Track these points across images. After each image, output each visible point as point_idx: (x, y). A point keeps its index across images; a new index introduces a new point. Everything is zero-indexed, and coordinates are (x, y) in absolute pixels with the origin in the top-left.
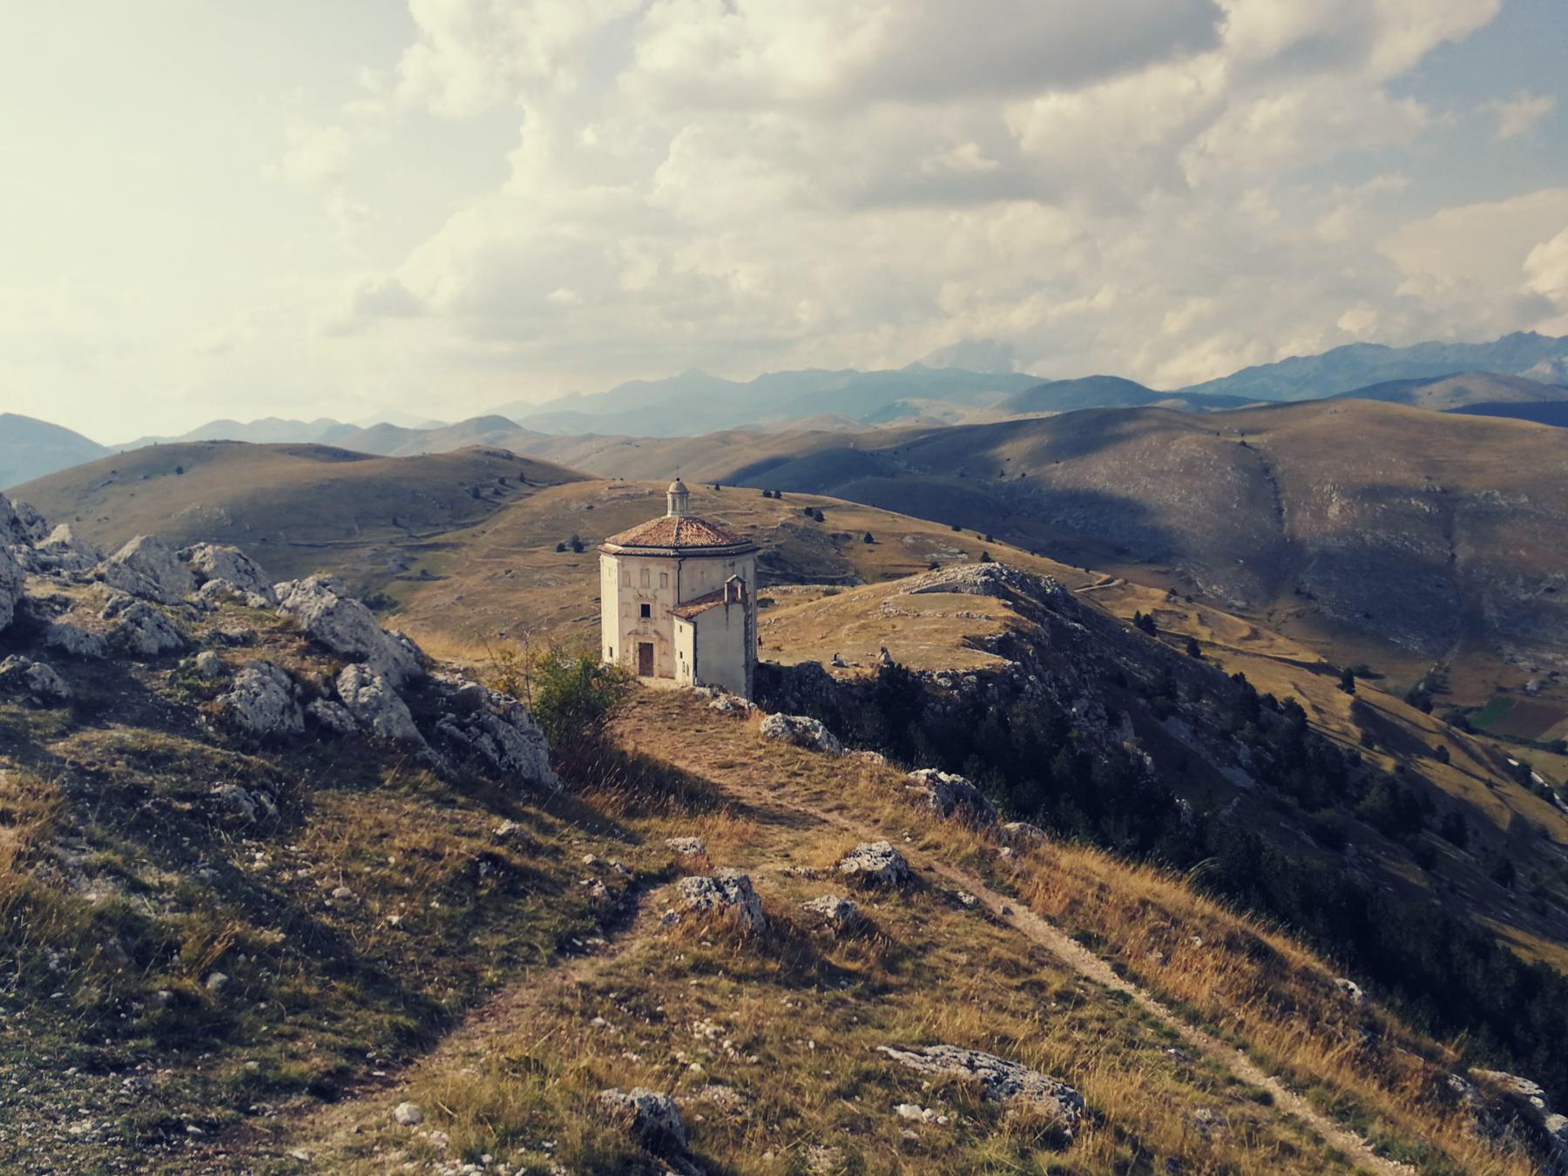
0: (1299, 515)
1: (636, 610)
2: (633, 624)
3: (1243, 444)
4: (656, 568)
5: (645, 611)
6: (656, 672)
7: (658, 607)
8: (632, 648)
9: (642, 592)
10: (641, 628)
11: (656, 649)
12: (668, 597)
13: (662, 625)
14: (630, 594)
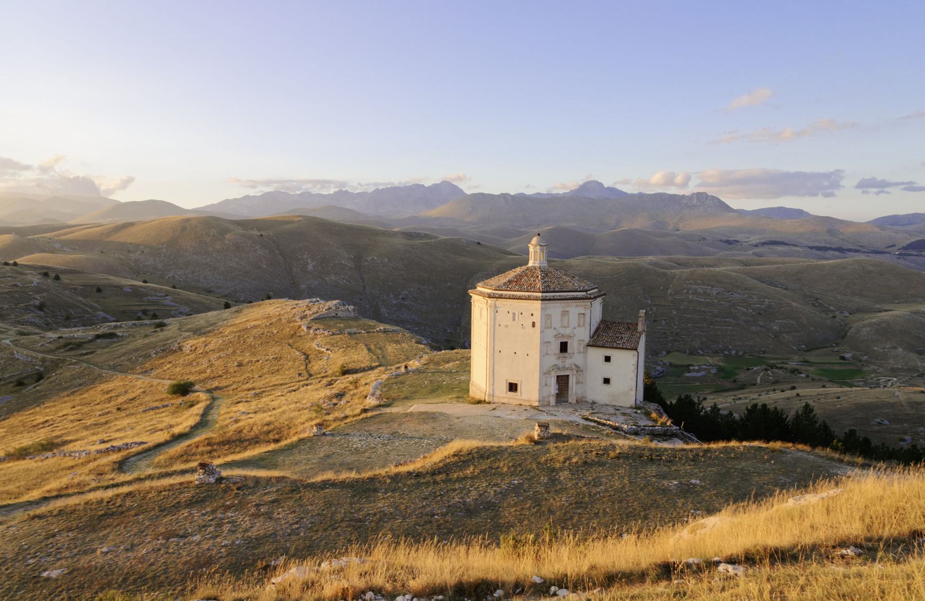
0: (294, 270)
1: (556, 347)
2: (553, 359)
3: (261, 235)
4: (575, 309)
5: (564, 347)
6: (572, 399)
8: (553, 381)
9: (562, 331)
10: (559, 363)
11: (572, 381)
12: (584, 334)
14: (550, 333)
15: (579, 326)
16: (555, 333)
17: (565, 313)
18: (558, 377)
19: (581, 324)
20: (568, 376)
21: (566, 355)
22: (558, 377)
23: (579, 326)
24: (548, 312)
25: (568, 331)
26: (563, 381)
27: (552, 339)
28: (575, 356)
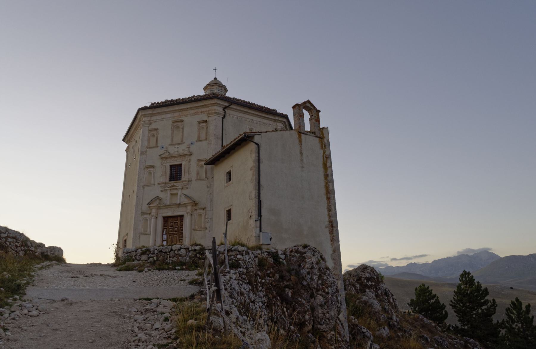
1: (162, 173)
5: (175, 173)
7: (194, 163)
8: (155, 225)
9: (173, 150)
10: (166, 197)
13: (197, 190)
15: (199, 140)
16: (162, 151)
17: (178, 124)
18: (166, 219)
19: (203, 136)
20: (182, 216)
21: (178, 184)
22: (166, 219)
23: (199, 140)
24: (153, 126)
25: (182, 149)
26: (173, 225)
27: (158, 163)
28: (194, 186)
